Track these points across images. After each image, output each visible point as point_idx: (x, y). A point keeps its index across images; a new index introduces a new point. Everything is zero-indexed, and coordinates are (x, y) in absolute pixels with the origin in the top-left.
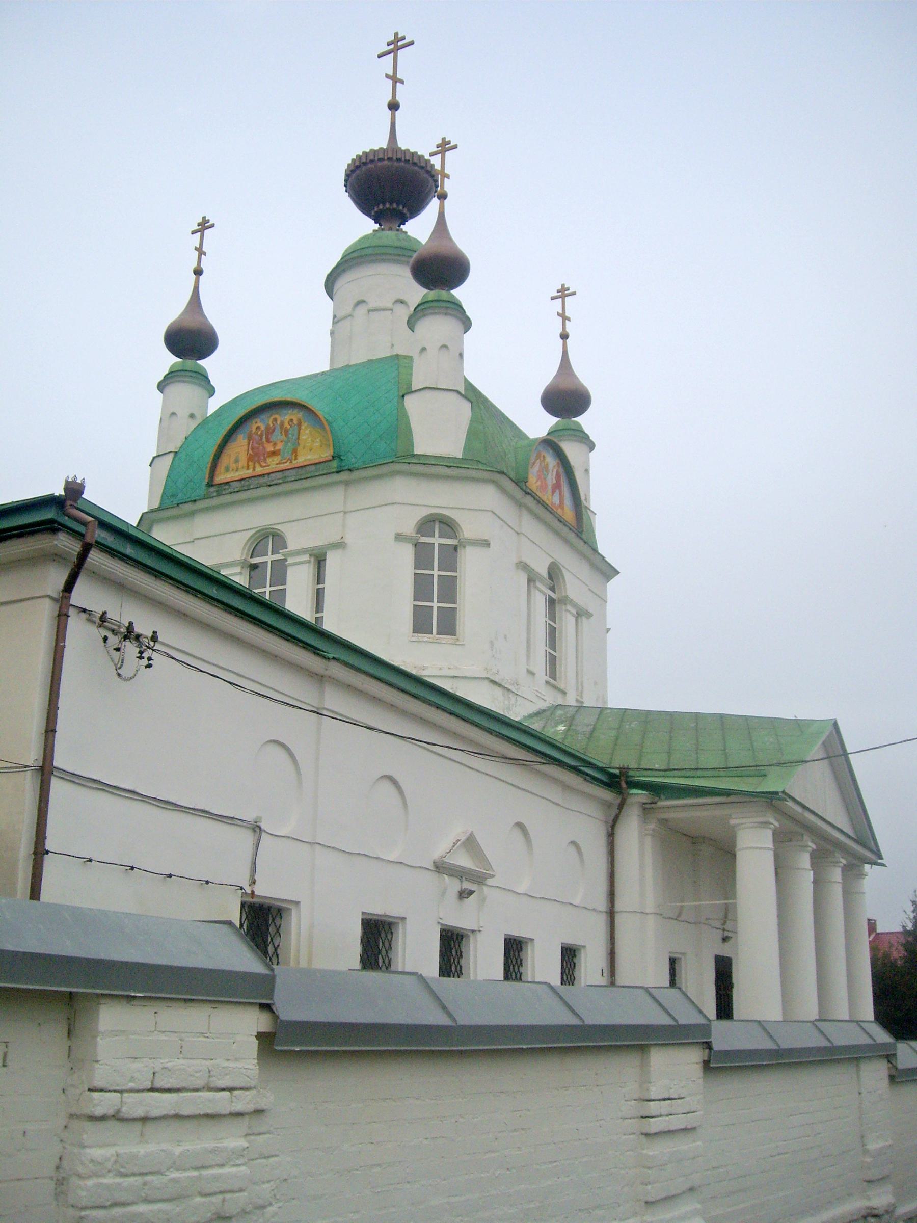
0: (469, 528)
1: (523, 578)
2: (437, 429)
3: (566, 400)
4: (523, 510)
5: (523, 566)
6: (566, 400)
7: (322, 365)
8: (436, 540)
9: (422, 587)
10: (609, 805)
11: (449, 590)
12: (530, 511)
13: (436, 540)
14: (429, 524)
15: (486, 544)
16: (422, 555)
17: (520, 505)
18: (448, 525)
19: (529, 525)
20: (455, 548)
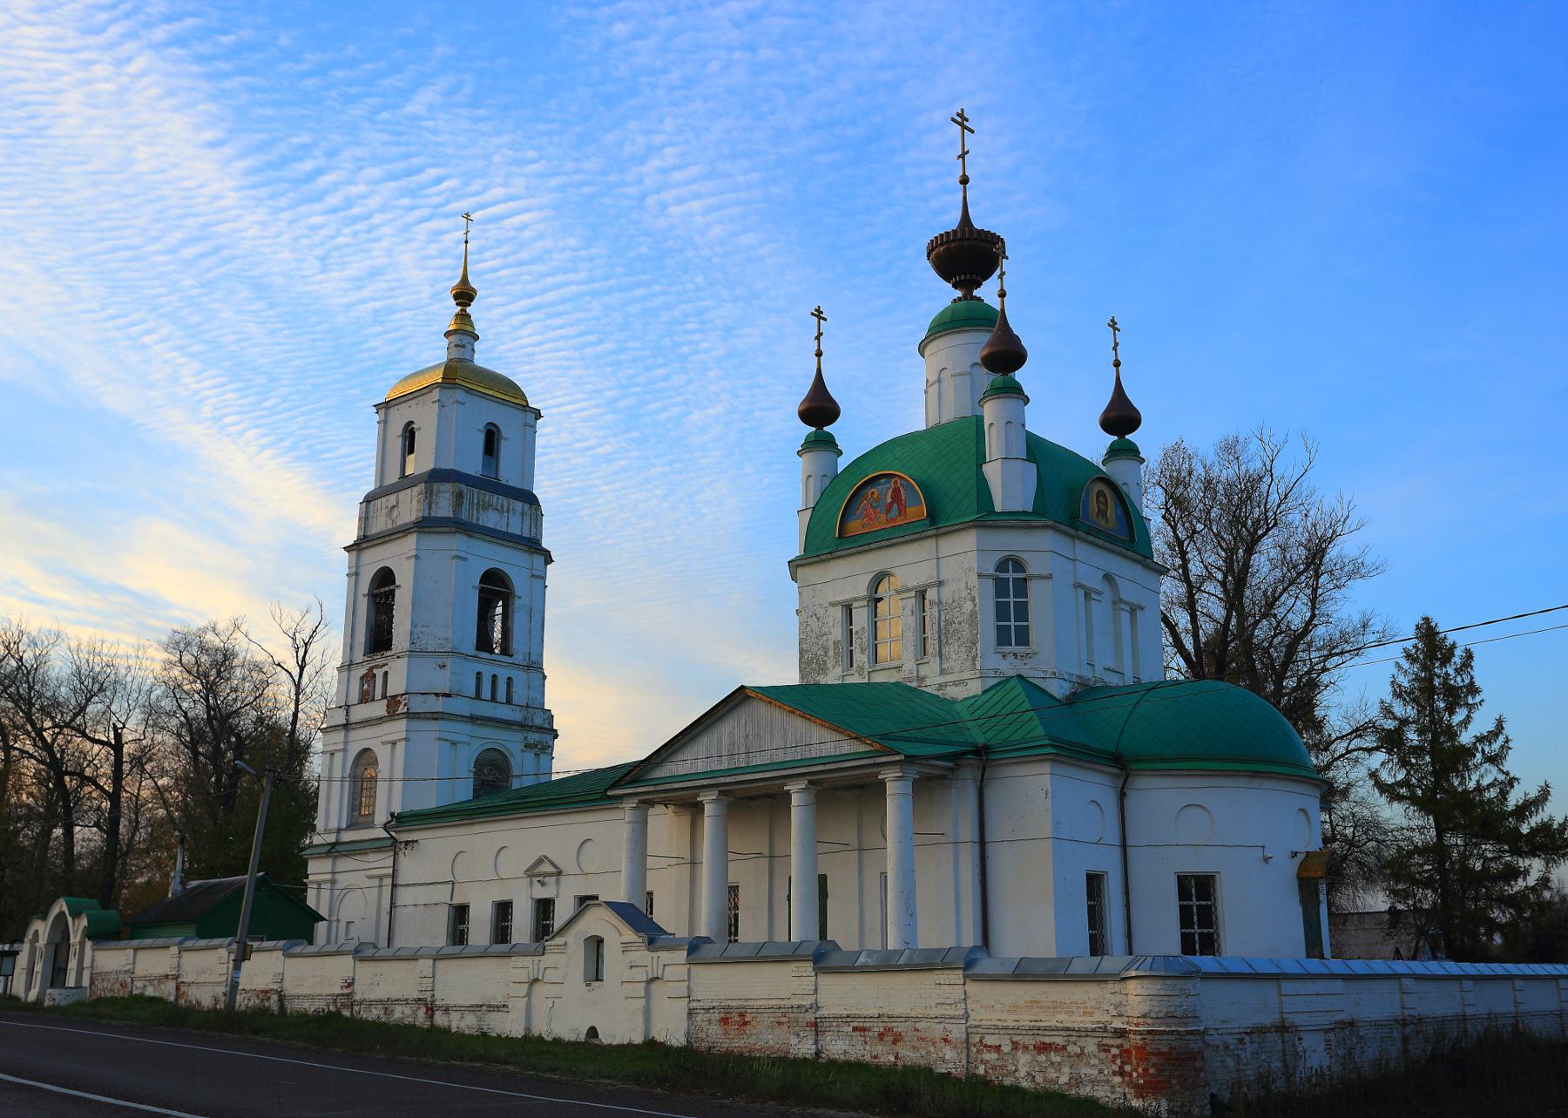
0: (1034, 565)
1: (1081, 592)
2: (1008, 484)
3: (1121, 418)
4: (1077, 542)
5: (1078, 586)
6: (1121, 418)
7: (916, 421)
8: (1011, 575)
9: (1002, 612)
10: (1118, 776)
11: (1022, 612)
12: (1083, 540)
13: (1011, 575)
14: (1002, 566)
15: (1050, 577)
16: (1001, 588)
17: (1073, 537)
18: (1019, 566)
19: (1083, 551)
20: (1025, 580)
